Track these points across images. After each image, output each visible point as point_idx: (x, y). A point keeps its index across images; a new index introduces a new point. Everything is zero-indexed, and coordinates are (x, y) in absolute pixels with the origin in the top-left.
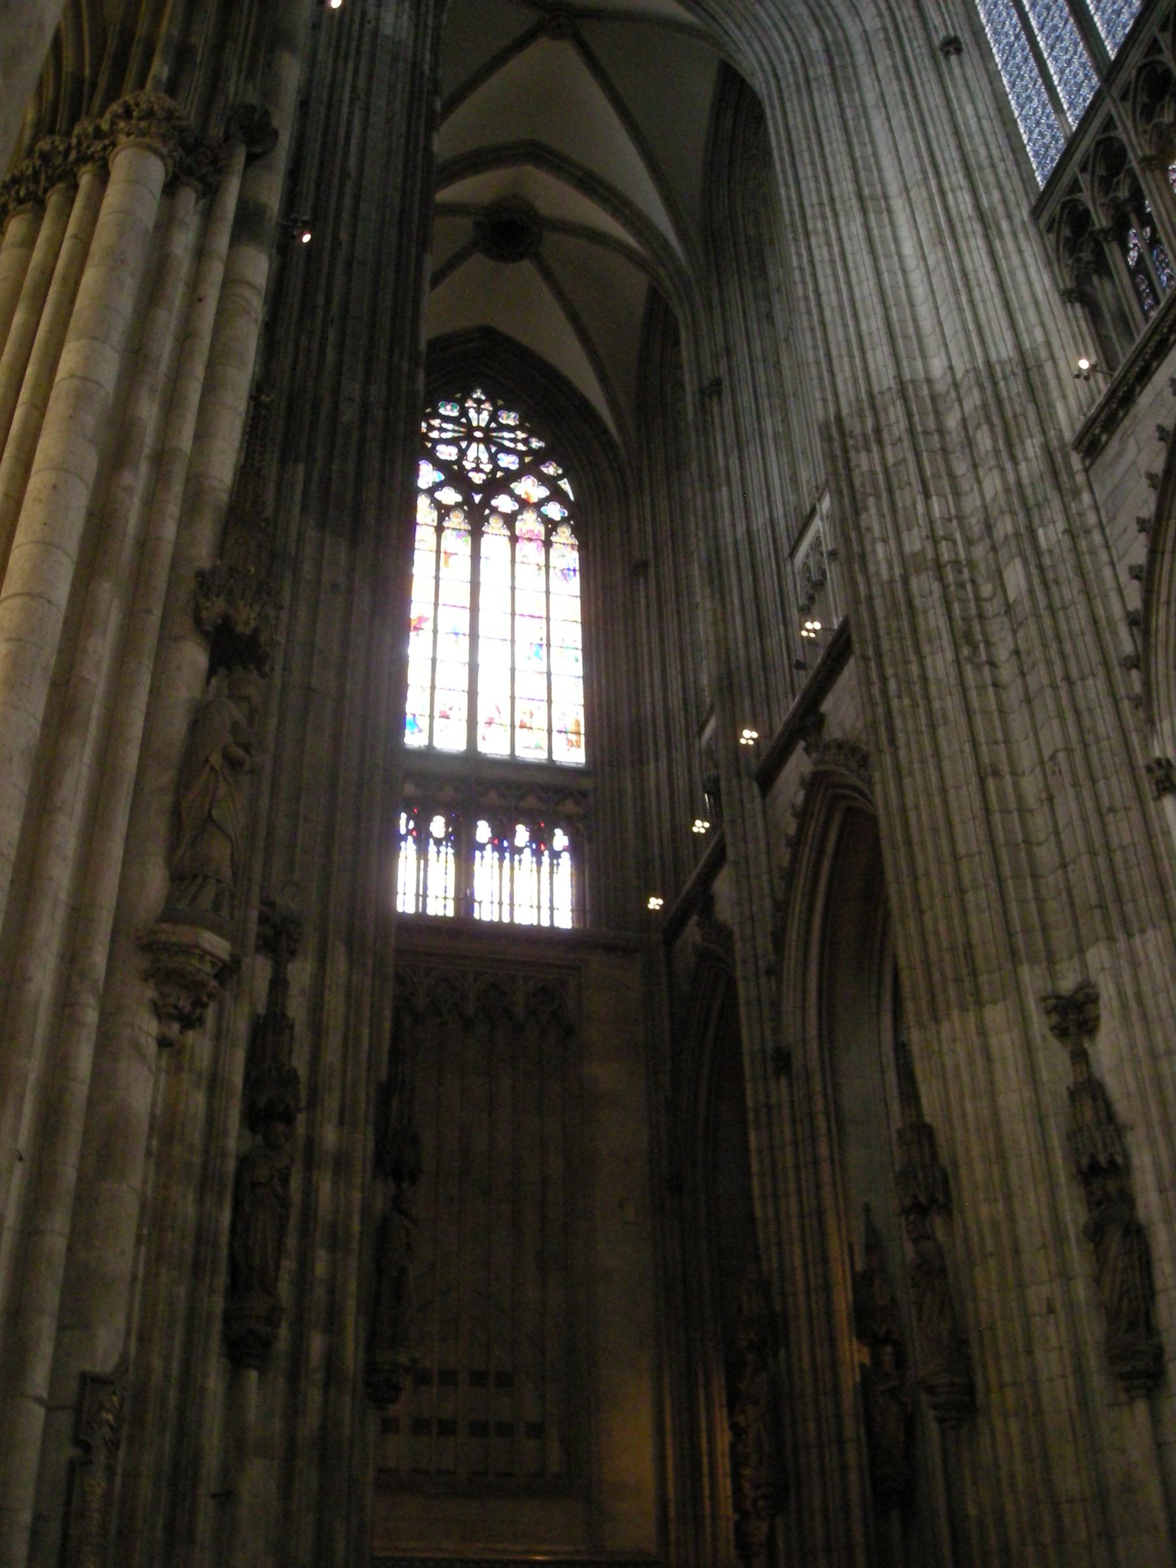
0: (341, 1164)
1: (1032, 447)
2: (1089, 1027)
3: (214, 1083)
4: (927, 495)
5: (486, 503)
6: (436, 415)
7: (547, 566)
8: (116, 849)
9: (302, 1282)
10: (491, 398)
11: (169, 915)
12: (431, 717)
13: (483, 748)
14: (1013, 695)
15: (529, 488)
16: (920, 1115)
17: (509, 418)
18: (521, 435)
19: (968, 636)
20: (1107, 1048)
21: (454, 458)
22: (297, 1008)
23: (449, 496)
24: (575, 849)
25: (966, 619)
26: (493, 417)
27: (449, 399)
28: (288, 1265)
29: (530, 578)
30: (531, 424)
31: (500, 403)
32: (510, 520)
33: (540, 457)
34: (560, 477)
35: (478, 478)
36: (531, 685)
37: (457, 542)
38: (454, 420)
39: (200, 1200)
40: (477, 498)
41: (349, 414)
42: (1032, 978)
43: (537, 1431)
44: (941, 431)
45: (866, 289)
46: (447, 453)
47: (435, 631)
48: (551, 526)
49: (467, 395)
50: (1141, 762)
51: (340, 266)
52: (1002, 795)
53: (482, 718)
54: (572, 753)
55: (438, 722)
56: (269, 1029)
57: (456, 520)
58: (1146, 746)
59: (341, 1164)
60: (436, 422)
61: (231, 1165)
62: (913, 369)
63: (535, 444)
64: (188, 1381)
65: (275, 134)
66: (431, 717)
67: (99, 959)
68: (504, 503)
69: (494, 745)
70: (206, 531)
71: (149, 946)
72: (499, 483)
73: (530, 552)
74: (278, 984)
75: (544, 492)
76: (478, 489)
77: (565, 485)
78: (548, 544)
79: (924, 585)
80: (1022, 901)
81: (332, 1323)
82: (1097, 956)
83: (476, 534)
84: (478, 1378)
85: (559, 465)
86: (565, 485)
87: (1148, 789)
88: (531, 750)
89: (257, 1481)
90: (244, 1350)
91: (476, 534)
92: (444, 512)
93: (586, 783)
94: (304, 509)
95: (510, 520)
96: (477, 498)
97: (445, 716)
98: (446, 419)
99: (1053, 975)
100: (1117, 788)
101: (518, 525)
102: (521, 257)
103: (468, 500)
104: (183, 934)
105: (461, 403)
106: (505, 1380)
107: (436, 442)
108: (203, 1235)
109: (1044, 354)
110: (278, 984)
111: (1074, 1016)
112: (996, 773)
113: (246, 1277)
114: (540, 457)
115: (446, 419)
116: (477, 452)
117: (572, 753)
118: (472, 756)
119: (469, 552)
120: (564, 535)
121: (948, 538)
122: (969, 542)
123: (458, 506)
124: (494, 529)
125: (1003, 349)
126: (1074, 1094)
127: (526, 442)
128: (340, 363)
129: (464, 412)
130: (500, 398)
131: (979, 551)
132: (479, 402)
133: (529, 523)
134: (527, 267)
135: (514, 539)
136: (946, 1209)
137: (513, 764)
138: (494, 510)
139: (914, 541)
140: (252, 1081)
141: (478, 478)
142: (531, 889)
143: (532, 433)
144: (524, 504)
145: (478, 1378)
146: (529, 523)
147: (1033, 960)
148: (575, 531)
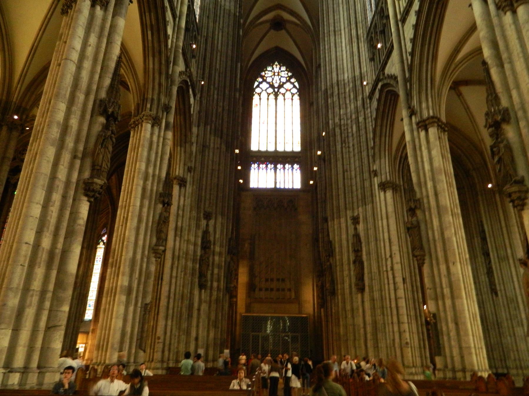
0: (220, 254)
1: (360, 98)
2: (358, 223)
3: (195, 245)
4: (340, 109)
5: (278, 91)
6: (266, 70)
8: (148, 237)
9: (212, 274)
10: (279, 64)
11: (156, 245)
14: (352, 154)
15: (288, 86)
16: (329, 239)
17: (283, 68)
19: (345, 141)
20: (361, 227)
22: (211, 229)
23: (270, 90)
24: (301, 168)
25: (345, 138)
26: (280, 69)
27: (269, 65)
28: (209, 272)
30: (289, 69)
32: (284, 95)
33: (290, 77)
35: (276, 85)
38: (271, 71)
39: (193, 264)
40: (276, 90)
41: (220, 110)
42: (349, 213)
43: (290, 290)
44: (345, 93)
45: (333, 57)
46: (269, 80)
48: (293, 95)
49: (274, 64)
50: (372, 170)
51: (217, 74)
52: (347, 175)
54: (297, 148)
56: (206, 233)
57: (272, 97)
58: (373, 166)
59: (220, 254)
61: (198, 257)
62: (341, 78)
63: (290, 74)
64: (191, 293)
65: (171, 107)
67: (146, 253)
68: (282, 90)
69: (280, 149)
70: (161, 186)
71: (153, 249)
72: (281, 86)
74: (207, 225)
75: (292, 86)
76: (276, 88)
79: (337, 130)
80: (349, 198)
81: (219, 281)
82: (360, 209)
83: (276, 99)
84: (278, 280)
85: (295, 78)
86: (296, 84)
87: (372, 176)
88: (289, 149)
89: (204, 307)
90: (202, 286)
91: (276, 99)
92: (269, 94)
93: (300, 155)
94: (210, 133)
95: (284, 95)
98: (269, 71)
99: (353, 212)
100: (366, 175)
102: (282, 29)
103: (274, 91)
104: (157, 248)
105: (272, 66)
106: (283, 280)
108: (193, 269)
109: (366, 74)
110: (207, 225)
111: (356, 220)
112: (347, 171)
113: (202, 275)
114: (290, 77)
115: (269, 71)
116: (276, 78)
117: (297, 148)
118: (276, 151)
120: (296, 98)
121: (344, 119)
122: (347, 119)
124: (280, 97)
125: (357, 73)
126: (353, 236)
128: (218, 99)
129: (273, 69)
130: (281, 64)
131: (349, 121)
132: (276, 65)
133: (288, 95)
134: (283, 31)
136: (332, 256)
137: (285, 152)
138: (280, 93)
139: (337, 120)
140: (202, 243)
141: (276, 85)
142: (291, 178)
143: (288, 72)
144: (287, 90)
145: (278, 280)
146: (288, 95)
147: (350, 210)
148: (299, 95)
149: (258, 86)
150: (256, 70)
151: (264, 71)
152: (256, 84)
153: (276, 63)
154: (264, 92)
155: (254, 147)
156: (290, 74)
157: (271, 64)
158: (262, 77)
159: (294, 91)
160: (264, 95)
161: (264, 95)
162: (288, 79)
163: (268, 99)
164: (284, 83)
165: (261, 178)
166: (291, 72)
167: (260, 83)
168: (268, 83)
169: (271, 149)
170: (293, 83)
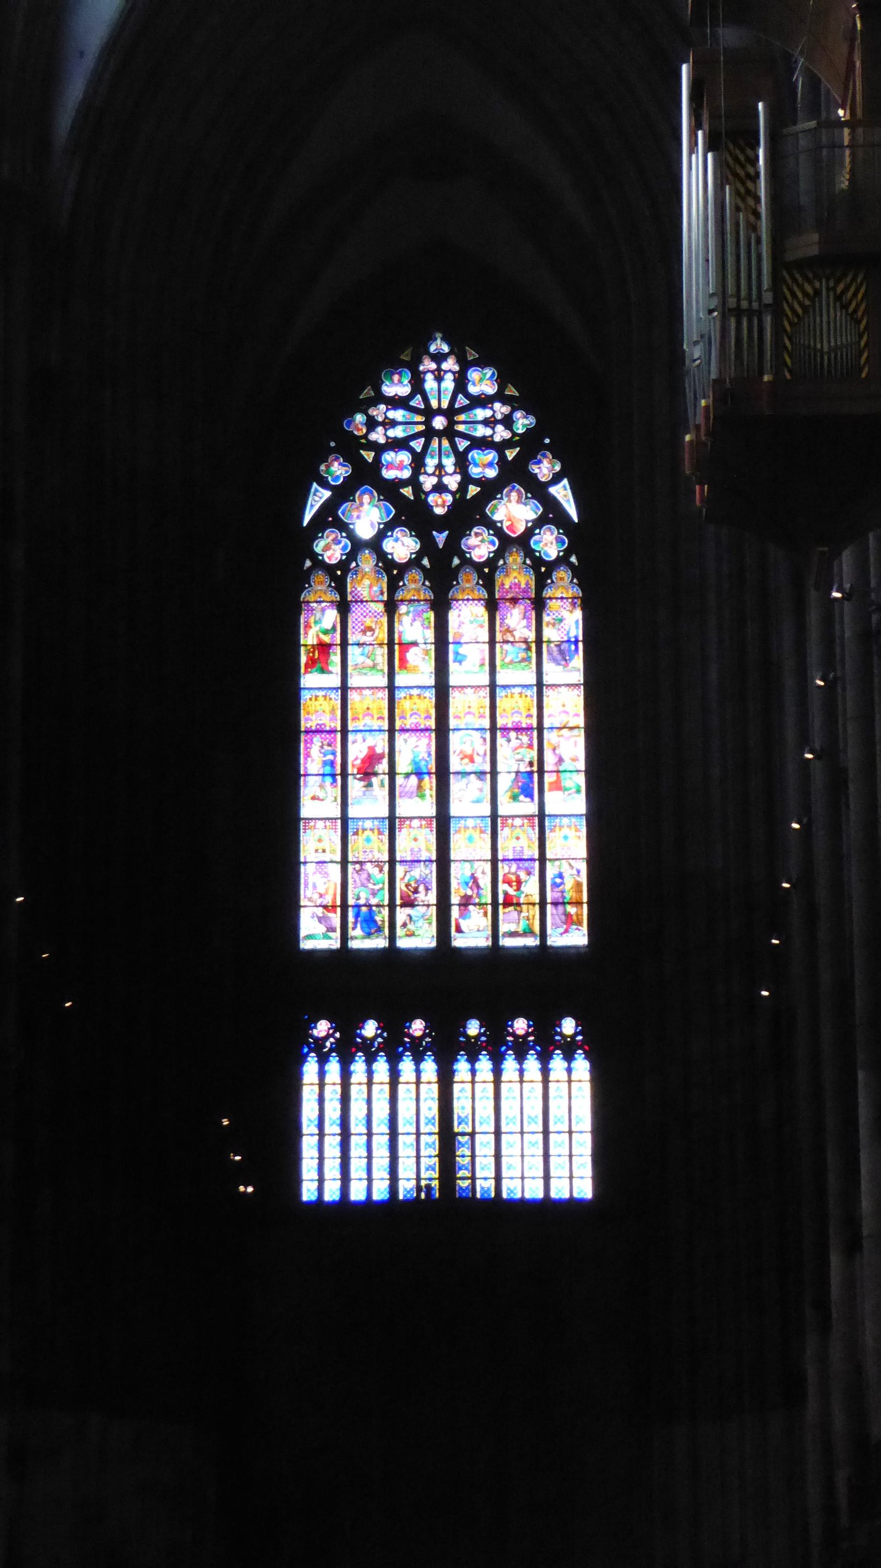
5: (454, 546)
7: (539, 641)
12: (392, 906)
13: (459, 942)
15: (514, 511)
17: (482, 382)
18: (500, 409)
21: (406, 474)
23: (402, 546)
27: (395, 365)
29: (516, 674)
31: (472, 355)
34: (556, 479)
35: (440, 505)
36: (518, 841)
37: (415, 627)
40: (441, 538)
47: (392, 773)
49: (421, 351)
53: (455, 899)
55: (401, 915)
57: (414, 586)
60: (379, 412)
63: (523, 422)
66: (392, 906)
68: (480, 546)
69: (472, 933)
73: (516, 620)
76: (441, 523)
77: (562, 493)
78: (539, 605)
88: (517, 933)
92: (393, 572)
95: (487, 573)
96: (441, 538)
97: (409, 903)
101: (499, 578)
103: (427, 547)
105: (413, 367)
107: (379, 449)
114: (530, 446)
119: (430, 635)
120: (563, 588)
123: (414, 562)
124: (468, 581)
127: (508, 422)
130: (473, 347)
133: (516, 576)
135: (492, 606)
141: (440, 505)
144: (506, 542)
146: (516, 576)
149: (329, 517)
150: (312, 418)
151: (364, 406)
152: (318, 497)
153: (439, 345)
154: (367, 562)
155: (315, 933)
156: (523, 422)
157: (407, 354)
158: (350, 448)
159: (549, 544)
160: (367, 584)
161: (367, 584)
162: (511, 454)
163: (391, 607)
164: (491, 490)
165: (362, 1130)
166: (528, 412)
167: (344, 493)
168: (389, 491)
169: (419, 935)
170: (537, 490)
